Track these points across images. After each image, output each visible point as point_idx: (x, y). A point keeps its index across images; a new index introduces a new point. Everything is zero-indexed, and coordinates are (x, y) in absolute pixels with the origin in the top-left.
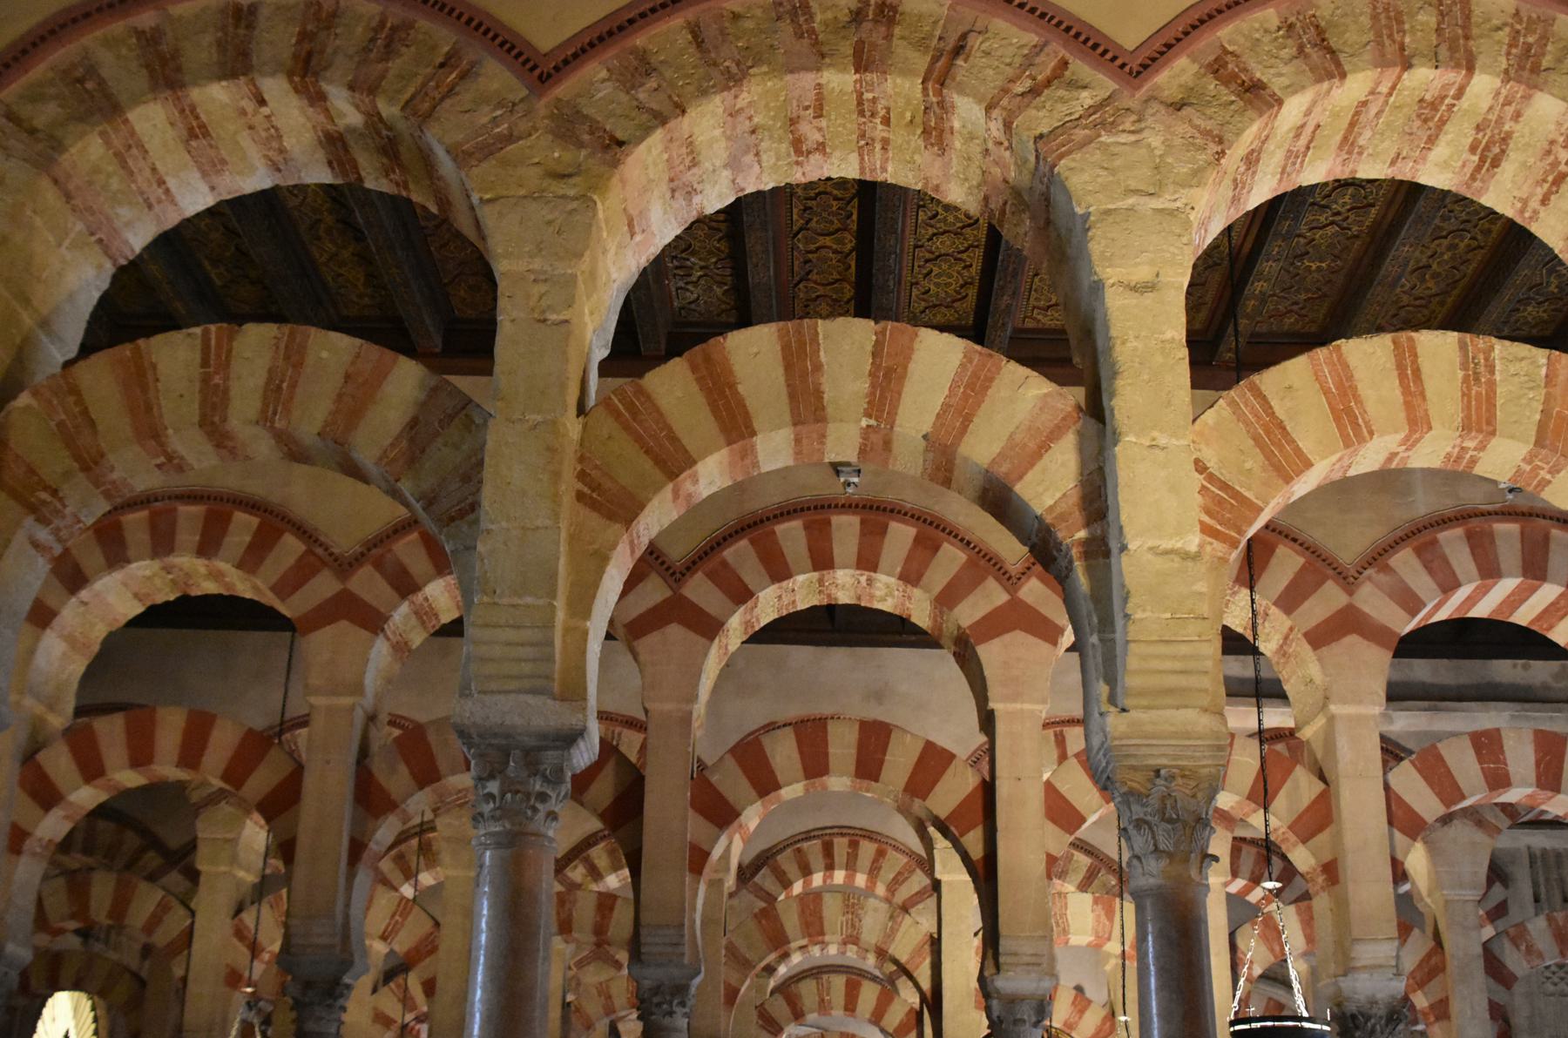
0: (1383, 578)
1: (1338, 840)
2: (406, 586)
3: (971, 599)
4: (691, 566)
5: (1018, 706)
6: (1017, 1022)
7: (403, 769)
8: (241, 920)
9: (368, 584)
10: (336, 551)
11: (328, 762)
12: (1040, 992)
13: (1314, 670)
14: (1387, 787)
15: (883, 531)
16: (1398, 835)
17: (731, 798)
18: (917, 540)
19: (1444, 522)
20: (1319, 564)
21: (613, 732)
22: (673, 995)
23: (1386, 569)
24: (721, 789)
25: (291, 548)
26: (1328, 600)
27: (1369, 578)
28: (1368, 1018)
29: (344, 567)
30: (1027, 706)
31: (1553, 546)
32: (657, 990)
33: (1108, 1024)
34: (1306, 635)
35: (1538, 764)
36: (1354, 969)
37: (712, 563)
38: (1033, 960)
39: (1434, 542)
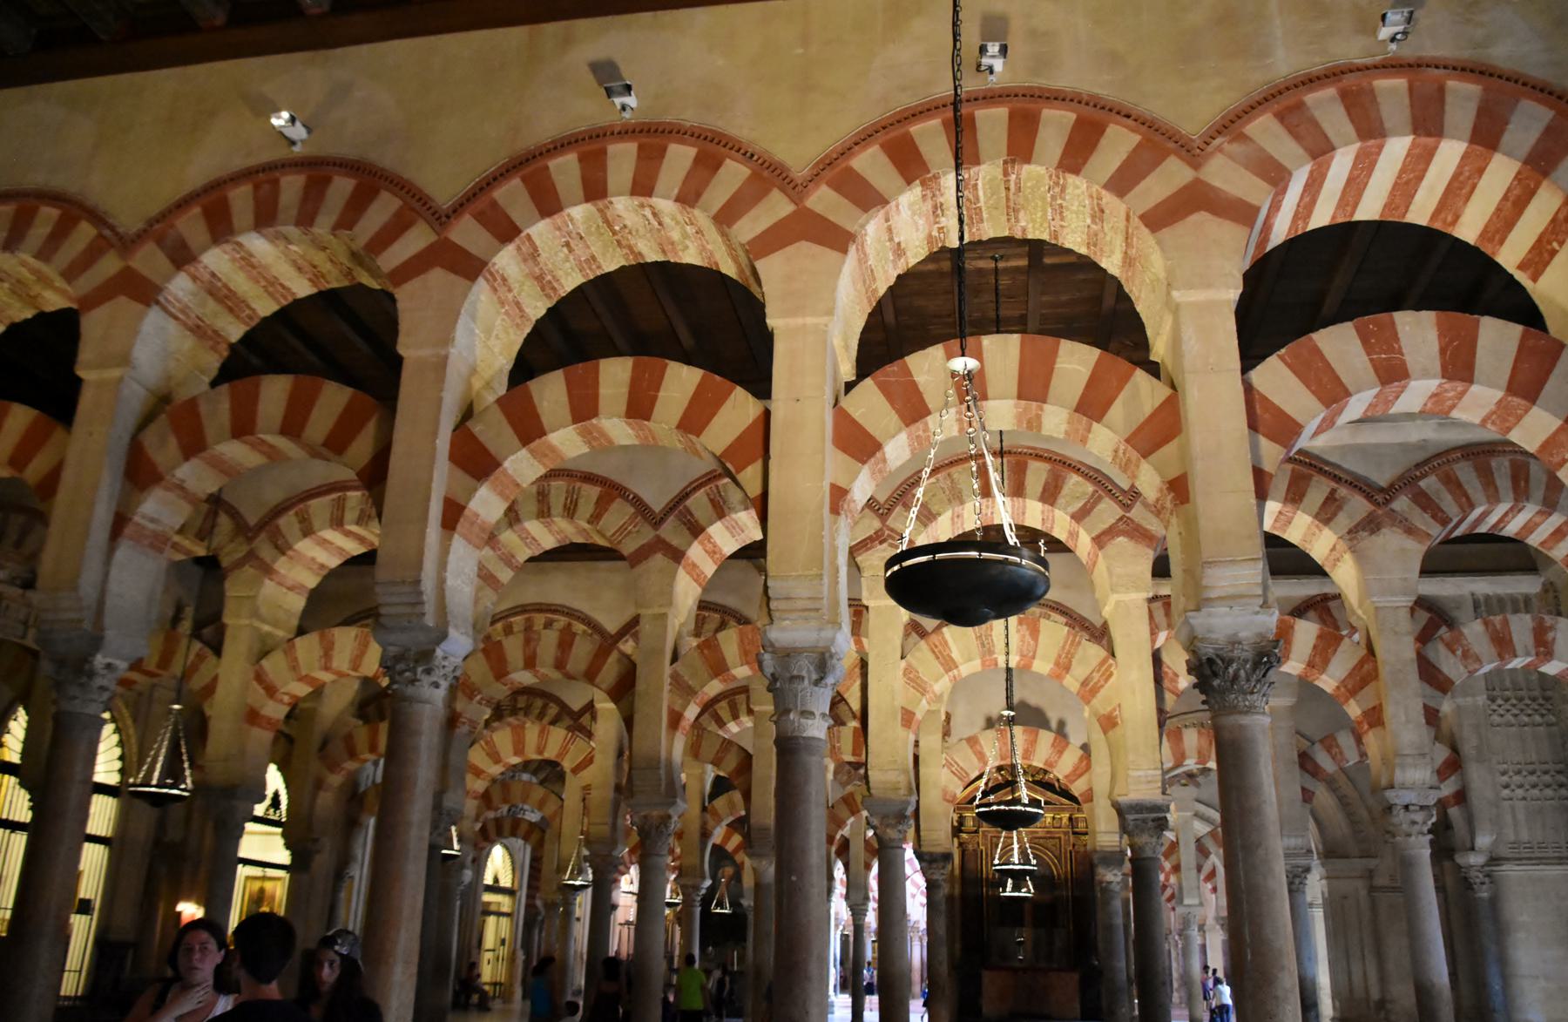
0: (1236, 148)
1: (1185, 455)
2: (182, 257)
3: (753, 213)
4: (458, 209)
5: (800, 321)
6: (793, 678)
7: (173, 442)
8: (261, 667)
9: (151, 259)
10: (121, 230)
11: (91, 434)
12: (821, 644)
13: (1157, 263)
14: (1249, 389)
15: (662, 151)
16: (1264, 442)
17: (492, 447)
18: (698, 161)
19: (1312, 81)
20: (1158, 138)
21: (574, 488)
22: (417, 661)
23: (1242, 138)
24: (482, 439)
25: (85, 232)
26: (1171, 176)
27: (1219, 149)
28: (1228, 662)
29: (127, 244)
30: (810, 320)
31: (1449, 99)
32: (399, 658)
33: (1085, 763)
34: (1143, 217)
35: (1443, 351)
36: (1208, 601)
37: (481, 204)
38: (810, 605)
39: (1300, 106)
